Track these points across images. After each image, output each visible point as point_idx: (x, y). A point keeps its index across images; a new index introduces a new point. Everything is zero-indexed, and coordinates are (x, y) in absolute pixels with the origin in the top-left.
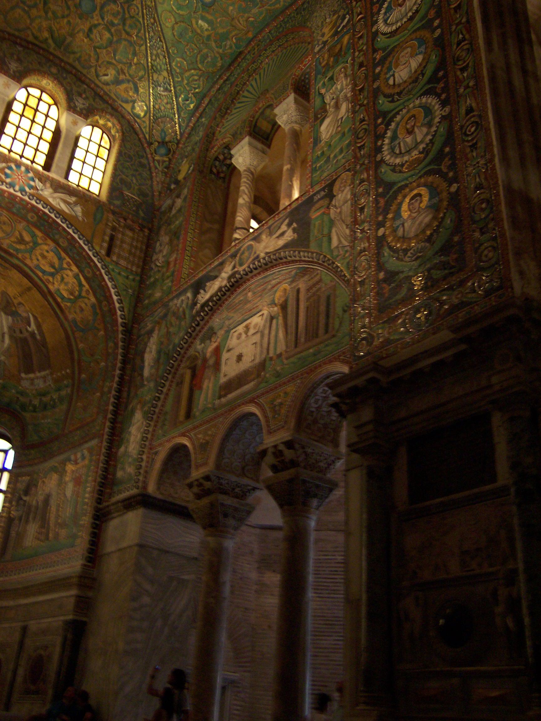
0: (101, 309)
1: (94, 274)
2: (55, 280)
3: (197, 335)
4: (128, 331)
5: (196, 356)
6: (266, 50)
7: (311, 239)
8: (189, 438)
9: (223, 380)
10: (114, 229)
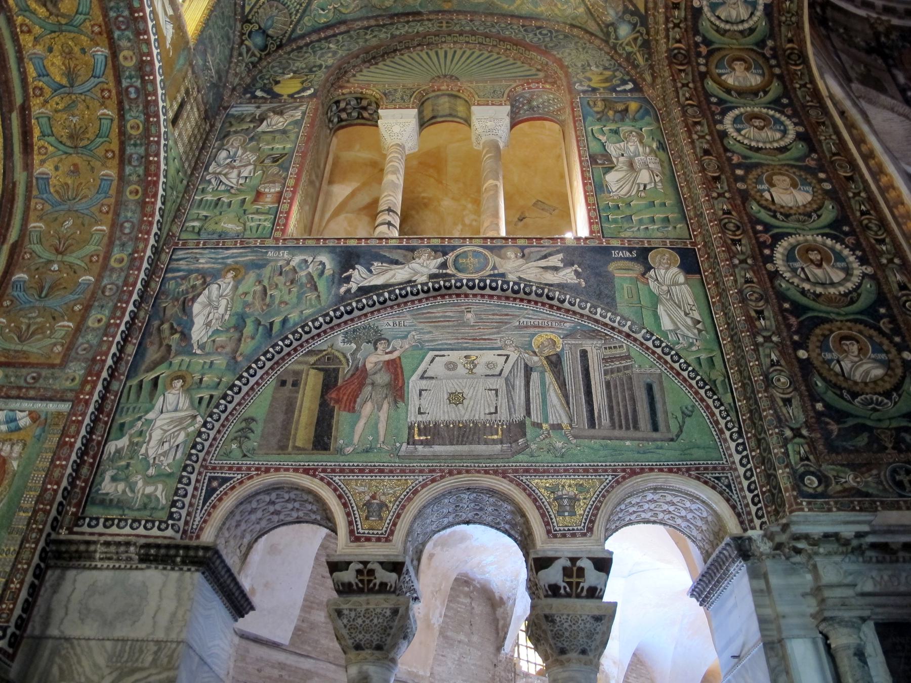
0: (120, 192)
1: (147, 133)
2: (57, 99)
3: (339, 325)
4: (157, 251)
5: (337, 357)
6: (461, 35)
7: (618, 300)
8: (329, 484)
9: (413, 417)
10: (187, 92)
